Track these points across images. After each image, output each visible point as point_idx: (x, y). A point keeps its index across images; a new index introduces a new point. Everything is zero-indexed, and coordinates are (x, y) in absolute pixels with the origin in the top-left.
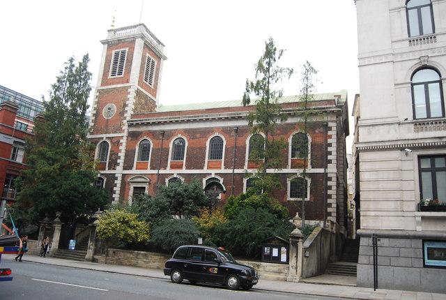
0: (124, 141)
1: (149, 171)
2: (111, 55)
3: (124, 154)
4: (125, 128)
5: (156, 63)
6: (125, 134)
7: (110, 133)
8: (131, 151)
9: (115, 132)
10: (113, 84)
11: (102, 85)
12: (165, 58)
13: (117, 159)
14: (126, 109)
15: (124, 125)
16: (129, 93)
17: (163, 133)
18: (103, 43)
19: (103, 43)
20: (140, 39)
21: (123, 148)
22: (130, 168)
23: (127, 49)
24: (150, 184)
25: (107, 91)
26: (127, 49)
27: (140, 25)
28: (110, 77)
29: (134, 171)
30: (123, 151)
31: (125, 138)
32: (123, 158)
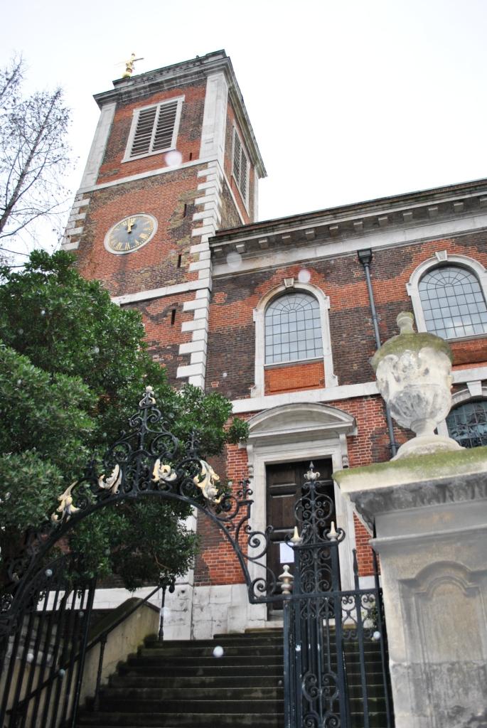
0: (199, 305)
1: (334, 390)
2: (130, 119)
3: (202, 346)
4: (201, 263)
5: (249, 164)
6: (204, 281)
7: (140, 290)
8: (243, 332)
9: (160, 284)
10: (138, 171)
11: (99, 181)
12: (263, 174)
13: (173, 367)
14: (196, 217)
15: (195, 258)
16: (204, 179)
17: (365, 259)
18: (101, 100)
19: (101, 100)
20: (222, 74)
21: (197, 328)
22: (244, 390)
23: (180, 100)
24: (351, 440)
25: (121, 190)
26: (180, 100)
27: (214, 54)
28: (127, 156)
29: (257, 401)
30: (200, 337)
31: (203, 295)
32: (199, 358)
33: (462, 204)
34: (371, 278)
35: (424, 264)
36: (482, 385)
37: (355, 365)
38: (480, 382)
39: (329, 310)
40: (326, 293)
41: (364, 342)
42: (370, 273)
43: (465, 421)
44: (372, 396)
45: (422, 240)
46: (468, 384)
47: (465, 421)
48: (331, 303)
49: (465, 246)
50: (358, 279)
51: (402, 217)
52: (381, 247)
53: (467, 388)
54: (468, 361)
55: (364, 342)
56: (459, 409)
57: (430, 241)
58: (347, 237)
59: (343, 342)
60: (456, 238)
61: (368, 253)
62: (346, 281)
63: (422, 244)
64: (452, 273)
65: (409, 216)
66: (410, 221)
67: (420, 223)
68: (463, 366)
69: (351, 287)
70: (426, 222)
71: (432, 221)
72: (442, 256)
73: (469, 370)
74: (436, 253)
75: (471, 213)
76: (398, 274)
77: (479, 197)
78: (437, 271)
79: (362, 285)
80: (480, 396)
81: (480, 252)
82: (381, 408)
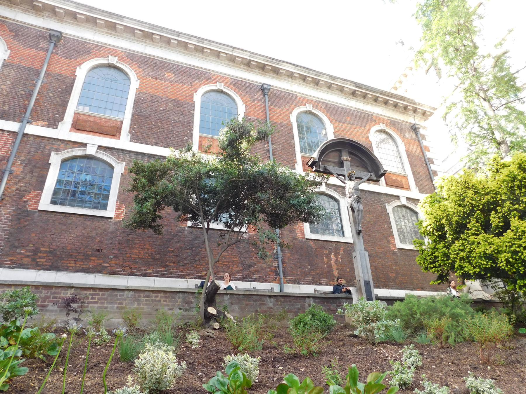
33: (141, 33)
34: (52, 53)
35: (98, 60)
36: (97, 149)
37: (7, 106)
38: (97, 146)
39: (5, 60)
40: (8, 47)
41: (23, 93)
42: (54, 49)
43: (76, 169)
44: (8, 131)
45: (105, 44)
46: (87, 145)
47: (76, 169)
48: (10, 56)
49: (132, 60)
50: (42, 49)
51: (96, 23)
52: (72, 35)
53: (86, 147)
54: (97, 131)
55: (23, 93)
56: (75, 160)
57: (110, 47)
58: (49, 17)
59: (5, 87)
60: (128, 53)
61: (58, 34)
62: (31, 47)
63: (104, 47)
64: (112, 72)
65: (102, 24)
66: (102, 28)
67: (108, 33)
68: (91, 133)
69: (33, 52)
70: (113, 35)
71: (117, 36)
72: (113, 60)
73: (93, 137)
74: (110, 56)
75: (145, 42)
76: (76, 58)
77: (153, 34)
78: (107, 69)
79: (42, 54)
80: (93, 155)
81: (139, 67)
82: (12, 142)
